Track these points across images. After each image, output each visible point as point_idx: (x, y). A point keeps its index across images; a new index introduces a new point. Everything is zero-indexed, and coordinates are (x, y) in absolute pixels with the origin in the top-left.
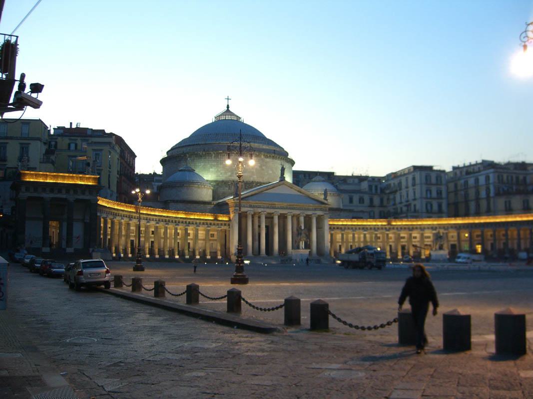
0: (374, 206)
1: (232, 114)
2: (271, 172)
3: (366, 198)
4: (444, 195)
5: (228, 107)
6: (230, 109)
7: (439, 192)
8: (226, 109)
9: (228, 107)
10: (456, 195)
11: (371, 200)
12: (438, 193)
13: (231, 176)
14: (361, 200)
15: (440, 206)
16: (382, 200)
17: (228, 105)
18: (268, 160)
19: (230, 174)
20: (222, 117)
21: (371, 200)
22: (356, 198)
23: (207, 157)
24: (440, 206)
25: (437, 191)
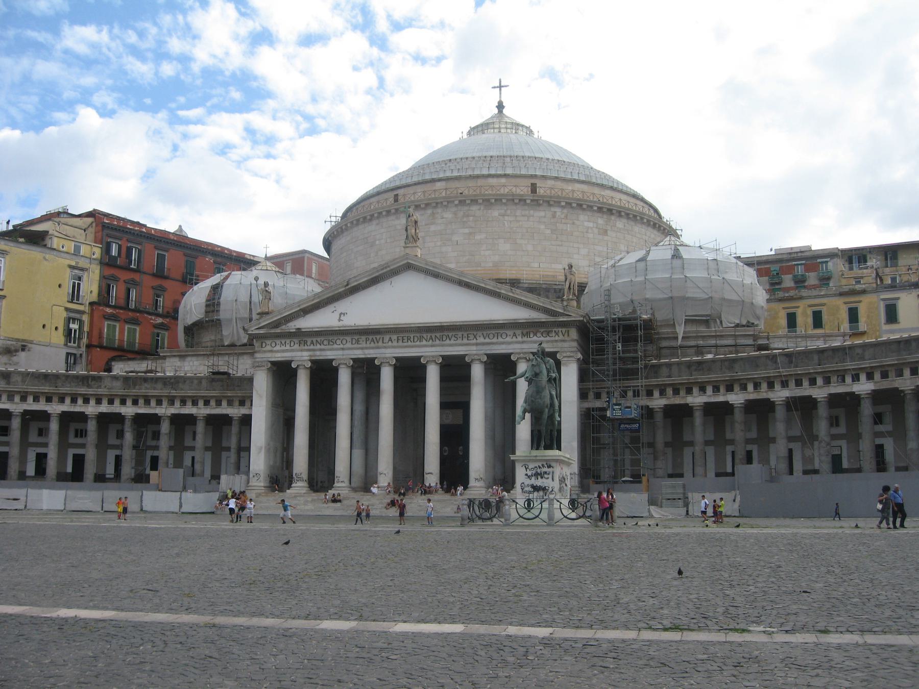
5: (500, 106)
6: (505, 111)
8: (496, 111)
9: (500, 106)
18: (495, 212)
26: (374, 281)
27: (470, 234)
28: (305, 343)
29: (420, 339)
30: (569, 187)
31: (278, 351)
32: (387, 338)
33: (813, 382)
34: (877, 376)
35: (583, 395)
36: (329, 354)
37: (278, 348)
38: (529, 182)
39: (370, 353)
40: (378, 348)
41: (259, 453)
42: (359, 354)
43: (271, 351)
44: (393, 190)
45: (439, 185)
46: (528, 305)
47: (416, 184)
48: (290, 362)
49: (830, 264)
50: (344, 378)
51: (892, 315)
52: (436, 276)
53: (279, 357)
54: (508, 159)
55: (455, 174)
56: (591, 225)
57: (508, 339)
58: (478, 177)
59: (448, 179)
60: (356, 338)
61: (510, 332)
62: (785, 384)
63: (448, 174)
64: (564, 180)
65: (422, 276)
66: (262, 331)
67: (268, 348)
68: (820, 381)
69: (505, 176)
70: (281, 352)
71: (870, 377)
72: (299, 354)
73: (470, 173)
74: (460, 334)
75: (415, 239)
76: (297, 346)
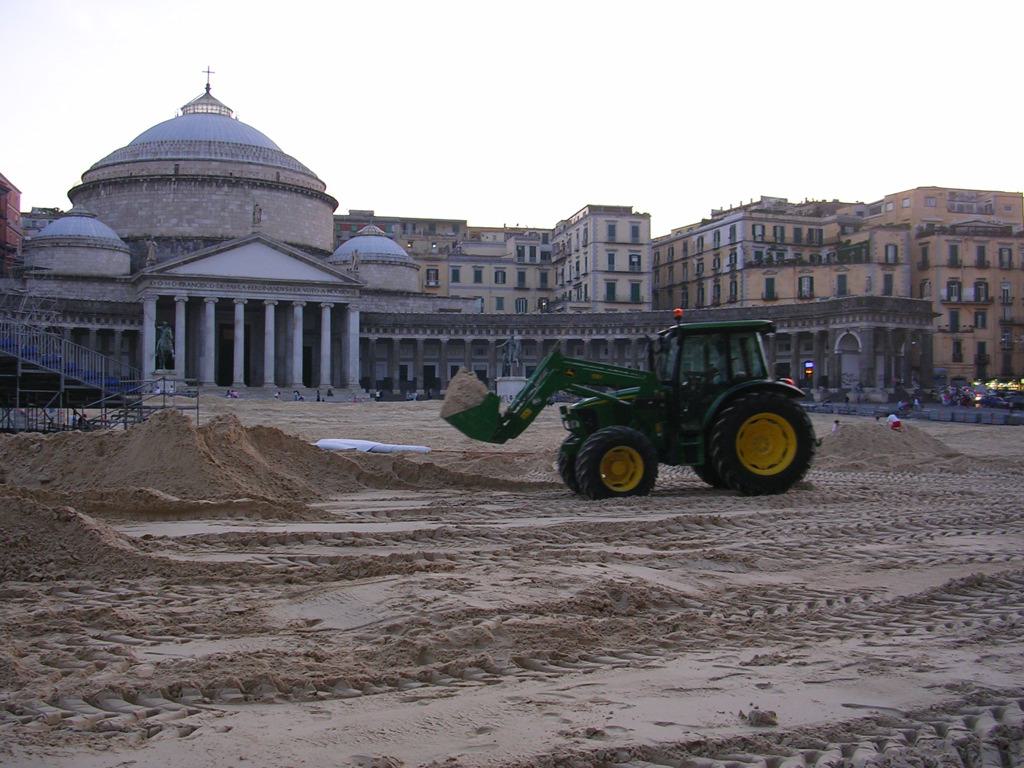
0: (528, 289)
1: (215, 103)
3: (512, 273)
4: (646, 265)
5: (208, 88)
6: (211, 92)
7: (635, 260)
8: (205, 92)
9: (208, 88)
10: (685, 265)
11: (522, 276)
12: (632, 263)
13: (177, 225)
14: (500, 277)
15: (635, 288)
16: (544, 278)
17: (208, 85)
19: (174, 221)
20: (200, 107)
21: (522, 276)
22: (488, 272)
23: (134, 189)
24: (635, 288)
25: (631, 257)
27: (241, 205)
29: (264, 288)
30: (297, 177)
32: (242, 285)
33: (488, 332)
34: (524, 332)
35: (361, 330)
36: (201, 294)
38: (275, 171)
39: (230, 295)
42: (223, 295)
43: (158, 288)
44: (174, 160)
45: (214, 163)
46: (331, 273)
47: (195, 160)
48: (174, 297)
49: (393, 227)
50: (211, 310)
51: (456, 276)
52: (275, 248)
53: (165, 292)
54: (254, 150)
55: (224, 158)
56: (309, 205)
58: (243, 163)
59: (221, 161)
61: (320, 289)
62: (472, 332)
63: (219, 157)
64: (295, 172)
66: (155, 274)
68: (492, 333)
69: (262, 165)
70: (166, 289)
71: (520, 333)
72: (179, 291)
73: (235, 159)
75: (260, 220)
76: (177, 286)
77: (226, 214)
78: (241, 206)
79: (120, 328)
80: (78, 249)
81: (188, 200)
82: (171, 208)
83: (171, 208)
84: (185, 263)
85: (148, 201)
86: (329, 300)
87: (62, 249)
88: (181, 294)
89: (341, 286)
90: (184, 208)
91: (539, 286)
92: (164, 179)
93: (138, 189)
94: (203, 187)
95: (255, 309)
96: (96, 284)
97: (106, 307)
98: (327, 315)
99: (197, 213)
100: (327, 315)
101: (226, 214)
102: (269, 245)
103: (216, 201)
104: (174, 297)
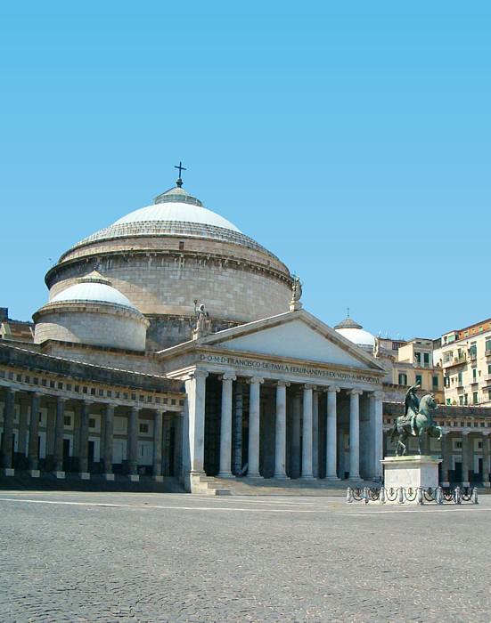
2: (262, 303)
18: (257, 277)
19: (182, 299)
26: (278, 324)
28: (232, 360)
31: (213, 364)
36: (248, 372)
37: (213, 361)
40: (280, 373)
41: (200, 445)
44: (179, 237)
45: (217, 244)
47: (200, 239)
48: (223, 374)
52: (314, 328)
57: (351, 379)
60: (266, 362)
65: (304, 326)
67: (206, 360)
72: (229, 369)
74: (326, 370)
77: (231, 296)
78: (244, 290)
79: (163, 408)
80: (106, 317)
81: (195, 279)
82: (178, 286)
83: (178, 286)
84: (234, 337)
85: (154, 277)
86: (357, 387)
87: (89, 315)
88: (230, 373)
89: (368, 373)
90: (192, 287)
91: (431, 389)
92: (173, 256)
93: (143, 264)
94: (210, 267)
95: (269, 390)
96: (124, 358)
97: (148, 382)
98: (355, 402)
99: (203, 292)
100: (355, 402)
101: (231, 296)
102: (308, 324)
103: (221, 283)
104: (223, 374)
